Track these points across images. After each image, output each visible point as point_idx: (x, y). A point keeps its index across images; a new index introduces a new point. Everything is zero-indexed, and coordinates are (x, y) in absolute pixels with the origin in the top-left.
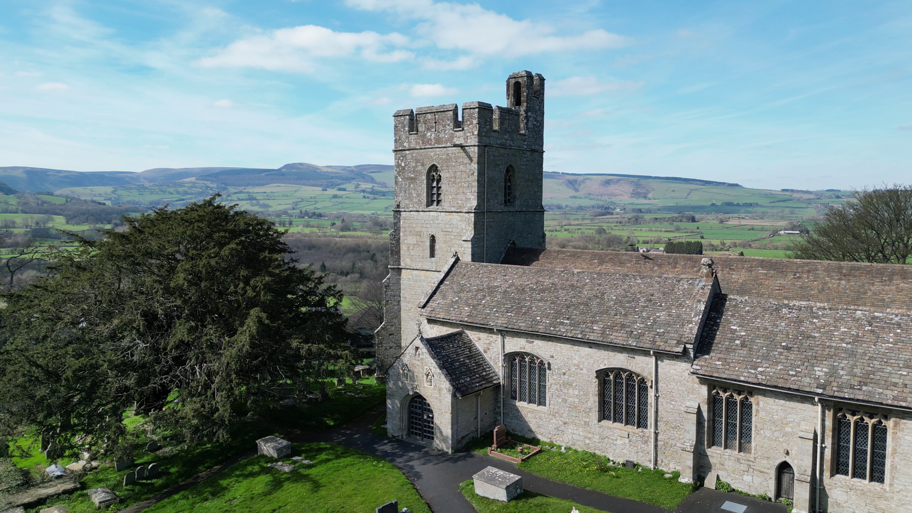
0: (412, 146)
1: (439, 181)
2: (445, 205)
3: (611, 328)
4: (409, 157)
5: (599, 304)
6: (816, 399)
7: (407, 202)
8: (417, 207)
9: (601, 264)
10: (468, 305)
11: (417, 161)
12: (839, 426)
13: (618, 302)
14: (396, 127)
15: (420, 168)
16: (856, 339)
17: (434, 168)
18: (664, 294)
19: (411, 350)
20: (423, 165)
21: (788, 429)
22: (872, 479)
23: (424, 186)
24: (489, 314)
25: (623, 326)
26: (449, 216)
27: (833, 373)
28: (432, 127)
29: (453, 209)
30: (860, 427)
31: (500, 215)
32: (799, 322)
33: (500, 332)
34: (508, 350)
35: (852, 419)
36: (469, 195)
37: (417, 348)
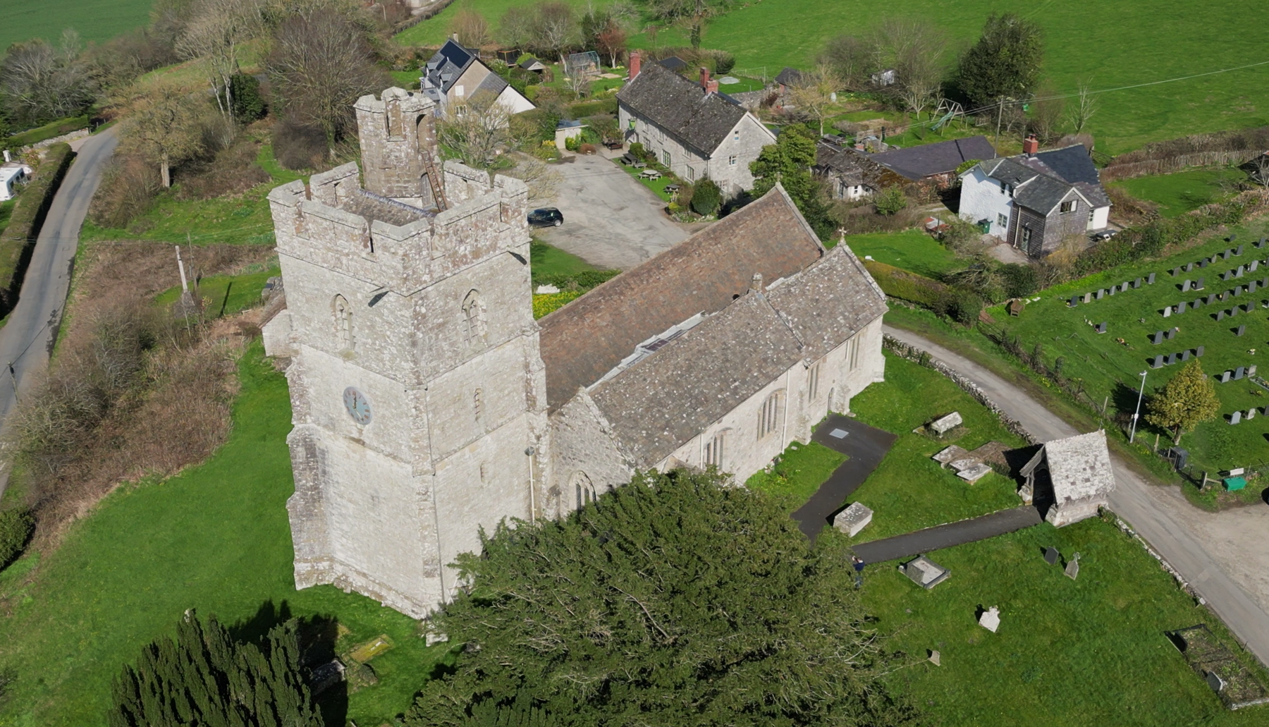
0: (436, 276)
3: (760, 367)
5: (734, 354)
7: (434, 363)
9: (582, 318)
10: (664, 430)
13: (741, 343)
15: (452, 303)
16: (830, 289)
18: (752, 318)
20: (456, 298)
24: (687, 423)
25: (765, 360)
27: (845, 318)
28: (467, 238)
32: (803, 293)
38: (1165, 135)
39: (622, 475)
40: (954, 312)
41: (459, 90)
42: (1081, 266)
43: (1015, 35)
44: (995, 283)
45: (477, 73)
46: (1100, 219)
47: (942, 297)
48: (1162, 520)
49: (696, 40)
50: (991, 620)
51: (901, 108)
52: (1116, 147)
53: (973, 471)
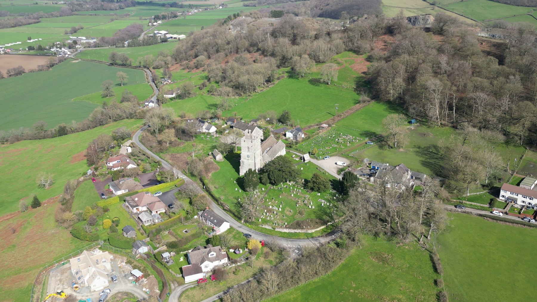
38: (309, 125)
39: (270, 160)
40: (290, 147)
41: (204, 127)
42: (302, 141)
43: (287, 113)
44: (294, 143)
45: (206, 124)
46: (303, 136)
47: (289, 146)
48: (314, 161)
49: (235, 115)
50: (302, 169)
51: (273, 124)
52: (303, 127)
53: (297, 159)
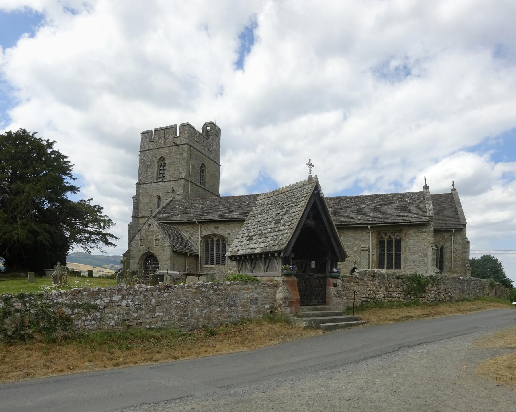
0: (150, 148)
1: (165, 165)
2: (168, 178)
4: (148, 154)
6: (369, 227)
8: (151, 181)
11: (153, 155)
12: (381, 243)
14: (142, 139)
17: (162, 158)
19: (146, 226)
20: (156, 157)
21: (356, 249)
22: (396, 268)
23: (156, 169)
26: (169, 184)
29: (172, 179)
30: (390, 242)
31: (198, 188)
33: (200, 223)
34: (205, 234)
35: (386, 238)
36: (181, 171)
37: (150, 225)
